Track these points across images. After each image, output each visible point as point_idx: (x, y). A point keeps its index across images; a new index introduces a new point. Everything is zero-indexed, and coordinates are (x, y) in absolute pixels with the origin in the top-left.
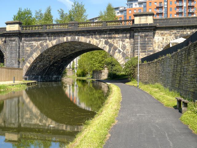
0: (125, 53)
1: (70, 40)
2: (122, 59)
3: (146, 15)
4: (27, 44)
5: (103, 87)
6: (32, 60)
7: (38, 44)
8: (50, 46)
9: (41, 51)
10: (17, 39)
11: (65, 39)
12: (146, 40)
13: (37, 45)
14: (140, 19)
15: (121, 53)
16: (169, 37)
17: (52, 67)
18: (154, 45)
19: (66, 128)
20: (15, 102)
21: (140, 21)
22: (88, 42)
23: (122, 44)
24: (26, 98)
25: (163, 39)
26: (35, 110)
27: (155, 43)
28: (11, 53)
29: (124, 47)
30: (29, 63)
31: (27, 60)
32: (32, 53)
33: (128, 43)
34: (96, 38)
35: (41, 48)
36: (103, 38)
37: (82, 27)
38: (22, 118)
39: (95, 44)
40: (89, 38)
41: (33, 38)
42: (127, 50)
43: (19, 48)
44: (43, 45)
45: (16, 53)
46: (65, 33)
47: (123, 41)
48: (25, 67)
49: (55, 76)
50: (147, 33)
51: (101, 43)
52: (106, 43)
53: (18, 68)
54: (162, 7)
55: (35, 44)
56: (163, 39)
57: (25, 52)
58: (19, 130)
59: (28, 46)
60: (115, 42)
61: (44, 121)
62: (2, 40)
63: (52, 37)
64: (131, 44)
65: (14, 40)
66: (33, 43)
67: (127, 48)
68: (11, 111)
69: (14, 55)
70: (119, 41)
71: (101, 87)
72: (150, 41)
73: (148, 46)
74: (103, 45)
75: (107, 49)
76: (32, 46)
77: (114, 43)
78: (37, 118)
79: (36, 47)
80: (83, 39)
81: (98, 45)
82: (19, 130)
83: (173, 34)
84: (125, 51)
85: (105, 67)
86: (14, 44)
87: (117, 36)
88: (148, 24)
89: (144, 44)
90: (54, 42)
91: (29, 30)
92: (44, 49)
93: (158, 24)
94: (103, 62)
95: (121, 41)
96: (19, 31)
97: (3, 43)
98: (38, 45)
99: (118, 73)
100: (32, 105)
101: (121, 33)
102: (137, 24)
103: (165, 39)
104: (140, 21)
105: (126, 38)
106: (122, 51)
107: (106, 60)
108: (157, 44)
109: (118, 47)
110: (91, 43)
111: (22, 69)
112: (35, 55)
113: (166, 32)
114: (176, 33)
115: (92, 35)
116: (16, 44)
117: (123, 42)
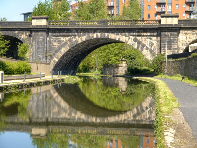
0: (152, 50)
1: (99, 37)
2: (150, 55)
3: (172, 17)
4: (54, 39)
5: (120, 84)
6: (60, 55)
7: (66, 39)
8: (80, 41)
9: (69, 47)
10: (44, 34)
11: (95, 36)
12: (172, 38)
13: (65, 40)
15: (149, 49)
16: (192, 36)
17: (72, 62)
18: (179, 43)
19: (96, 120)
20: (43, 97)
21: (166, 22)
22: (117, 39)
23: (150, 41)
24: (54, 93)
25: (187, 38)
26: (63, 104)
28: (38, 48)
29: (151, 45)
30: (57, 58)
31: (54, 55)
32: (60, 48)
33: (155, 41)
34: (126, 36)
35: (69, 43)
37: (110, 25)
38: (50, 112)
40: (119, 35)
41: (61, 34)
42: (155, 47)
44: (72, 41)
45: (44, 48)
46: (95, 30)
47: (151, 39)
48: (52, 62)
50: (172, 33)
51: (130, 40)
52: (135, 40)
53: (46, 64)
56: (187, 38)
57: (52, 46)
58: (46, 124)
59: (55, 41)
60: (143, 41)
61: (73, 115)
62: (26, 34)
63: (82, 33)
64: (158, 42)
65: (41, 35)
66: (61, 39)
67: (154, 45)
68: (38, 106)
69: (40, 50)
71: (117, 85)
72: (175, 40)
73: (173, 44)
74: (132, 42)
76: (59, 42)
77: (142, 40)
78: (66, 112)
79: (64, 44)
80: (112, 36)
81: (127, 42)
82: (46, 124)
83: (195, 33)
84: (152, 48)
85: (123, 60)
86: (40, 39)
87: (145, 34)
88: (173, 24)
89: (170, 42)
90: (84, 38)
91: (57, 25)
92: (73, 44)
93: (182, 25)
94: (119, 55)
96: (47, 26)
97: (27, 37)
98: (66, 41)
99: (139, 68)
100: (60, 100)
101: (149, 32)
102: (164, 25)
103: (188, 38)
104: (166, 22)
105: (154, 36)
106: (150, 48)
107: (124, 52)
108: (181, 42)
109: (146, 44)
110: (121, 40)
111: (49, 64)
112: (64, 50)
113: (189, 32)
115: (122, 33)
116: (44, 40)
117: (150, 40)
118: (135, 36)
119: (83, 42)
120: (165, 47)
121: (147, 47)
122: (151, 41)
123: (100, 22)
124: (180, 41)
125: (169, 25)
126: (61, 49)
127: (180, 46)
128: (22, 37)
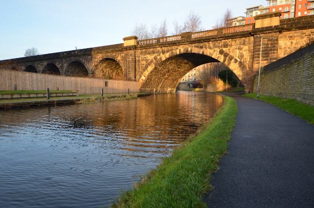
6: (147, 73)
8: (164, 59)
14: (263, 22)
16: (300, 40)
22: (201, 53)
25: (292, 43)
27: (281, 49)
29: (242, 56)
30: (145, 76)
31: (142, 73)
32: (146, 67)
34: (210, 48)
39: (208, 55)
42: (245, 59)
43: (135, 63)
47: (240, 49)
51: (215, 54)
52: (221, 52)
55: (150, 57)
56: (292, 43)
70: (236, 49)
75: (221, 59)
77: (230, 52)
87: (233, 43)
90: (167, 55)
93: (286, 26)
95: (238, 49)
105: (244, 44)
106: (239, 60)
109: (234, 56)
110: (205, 54)
112: (150, 69)
114: (310, 35)
118: (221, 47)
120: (259, 57)
122: (241, 51)
124: (281, 49)
126: (148, 67)
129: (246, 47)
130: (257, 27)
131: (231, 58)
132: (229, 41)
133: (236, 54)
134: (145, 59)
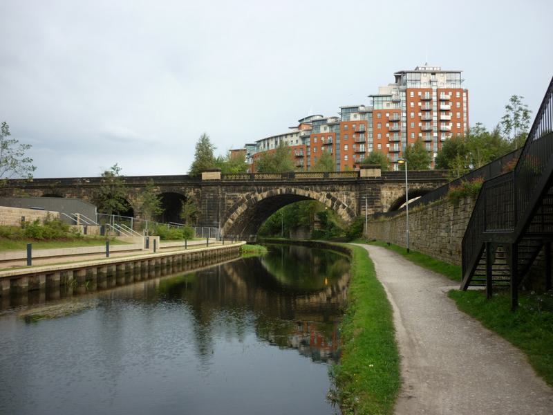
6: (235, 215)
8: (260, 198)
21: (367, 174)
22: (307, 195)
30: (233, 220)
31: (228, 215)
32: (235, 208)
34: (317, 191)
36: (326, 191)
46: (279, 184)
47: (348, 195)
49: (251, 236)
51: (322, 197)
52: (329, 196)
54: (398, 121)
55: (241, 196)
59: (229, 199)
76: (235, 199)
80: (300, 192)
81: (319, 199)
87: (341, 188)
90: (265, 195)
104: (367, 174)
105: (351, 190)
110: (311, 196)
112: (240, 210)
119: (264, 200)
121: (344, 205)
123: (283, 175)
125: (370, 178)
127: (385, 204)
128: (190, 194)
129: (353, 194)
130: (362, 176)
131: (339, 203)
132: (336, 187)
133: (343, 199)
134: (232, 197)
